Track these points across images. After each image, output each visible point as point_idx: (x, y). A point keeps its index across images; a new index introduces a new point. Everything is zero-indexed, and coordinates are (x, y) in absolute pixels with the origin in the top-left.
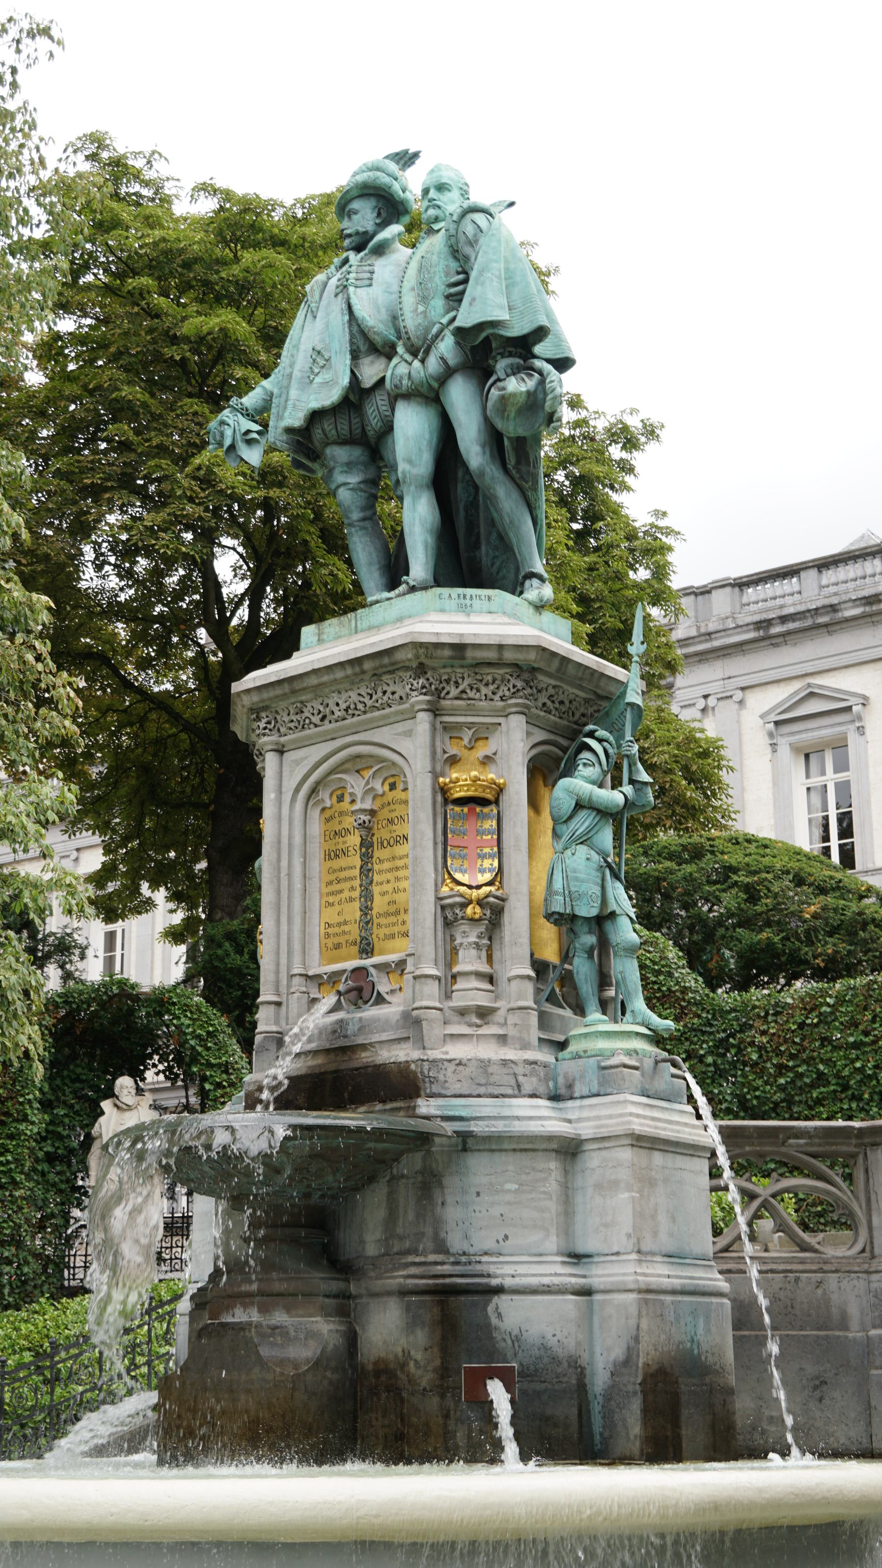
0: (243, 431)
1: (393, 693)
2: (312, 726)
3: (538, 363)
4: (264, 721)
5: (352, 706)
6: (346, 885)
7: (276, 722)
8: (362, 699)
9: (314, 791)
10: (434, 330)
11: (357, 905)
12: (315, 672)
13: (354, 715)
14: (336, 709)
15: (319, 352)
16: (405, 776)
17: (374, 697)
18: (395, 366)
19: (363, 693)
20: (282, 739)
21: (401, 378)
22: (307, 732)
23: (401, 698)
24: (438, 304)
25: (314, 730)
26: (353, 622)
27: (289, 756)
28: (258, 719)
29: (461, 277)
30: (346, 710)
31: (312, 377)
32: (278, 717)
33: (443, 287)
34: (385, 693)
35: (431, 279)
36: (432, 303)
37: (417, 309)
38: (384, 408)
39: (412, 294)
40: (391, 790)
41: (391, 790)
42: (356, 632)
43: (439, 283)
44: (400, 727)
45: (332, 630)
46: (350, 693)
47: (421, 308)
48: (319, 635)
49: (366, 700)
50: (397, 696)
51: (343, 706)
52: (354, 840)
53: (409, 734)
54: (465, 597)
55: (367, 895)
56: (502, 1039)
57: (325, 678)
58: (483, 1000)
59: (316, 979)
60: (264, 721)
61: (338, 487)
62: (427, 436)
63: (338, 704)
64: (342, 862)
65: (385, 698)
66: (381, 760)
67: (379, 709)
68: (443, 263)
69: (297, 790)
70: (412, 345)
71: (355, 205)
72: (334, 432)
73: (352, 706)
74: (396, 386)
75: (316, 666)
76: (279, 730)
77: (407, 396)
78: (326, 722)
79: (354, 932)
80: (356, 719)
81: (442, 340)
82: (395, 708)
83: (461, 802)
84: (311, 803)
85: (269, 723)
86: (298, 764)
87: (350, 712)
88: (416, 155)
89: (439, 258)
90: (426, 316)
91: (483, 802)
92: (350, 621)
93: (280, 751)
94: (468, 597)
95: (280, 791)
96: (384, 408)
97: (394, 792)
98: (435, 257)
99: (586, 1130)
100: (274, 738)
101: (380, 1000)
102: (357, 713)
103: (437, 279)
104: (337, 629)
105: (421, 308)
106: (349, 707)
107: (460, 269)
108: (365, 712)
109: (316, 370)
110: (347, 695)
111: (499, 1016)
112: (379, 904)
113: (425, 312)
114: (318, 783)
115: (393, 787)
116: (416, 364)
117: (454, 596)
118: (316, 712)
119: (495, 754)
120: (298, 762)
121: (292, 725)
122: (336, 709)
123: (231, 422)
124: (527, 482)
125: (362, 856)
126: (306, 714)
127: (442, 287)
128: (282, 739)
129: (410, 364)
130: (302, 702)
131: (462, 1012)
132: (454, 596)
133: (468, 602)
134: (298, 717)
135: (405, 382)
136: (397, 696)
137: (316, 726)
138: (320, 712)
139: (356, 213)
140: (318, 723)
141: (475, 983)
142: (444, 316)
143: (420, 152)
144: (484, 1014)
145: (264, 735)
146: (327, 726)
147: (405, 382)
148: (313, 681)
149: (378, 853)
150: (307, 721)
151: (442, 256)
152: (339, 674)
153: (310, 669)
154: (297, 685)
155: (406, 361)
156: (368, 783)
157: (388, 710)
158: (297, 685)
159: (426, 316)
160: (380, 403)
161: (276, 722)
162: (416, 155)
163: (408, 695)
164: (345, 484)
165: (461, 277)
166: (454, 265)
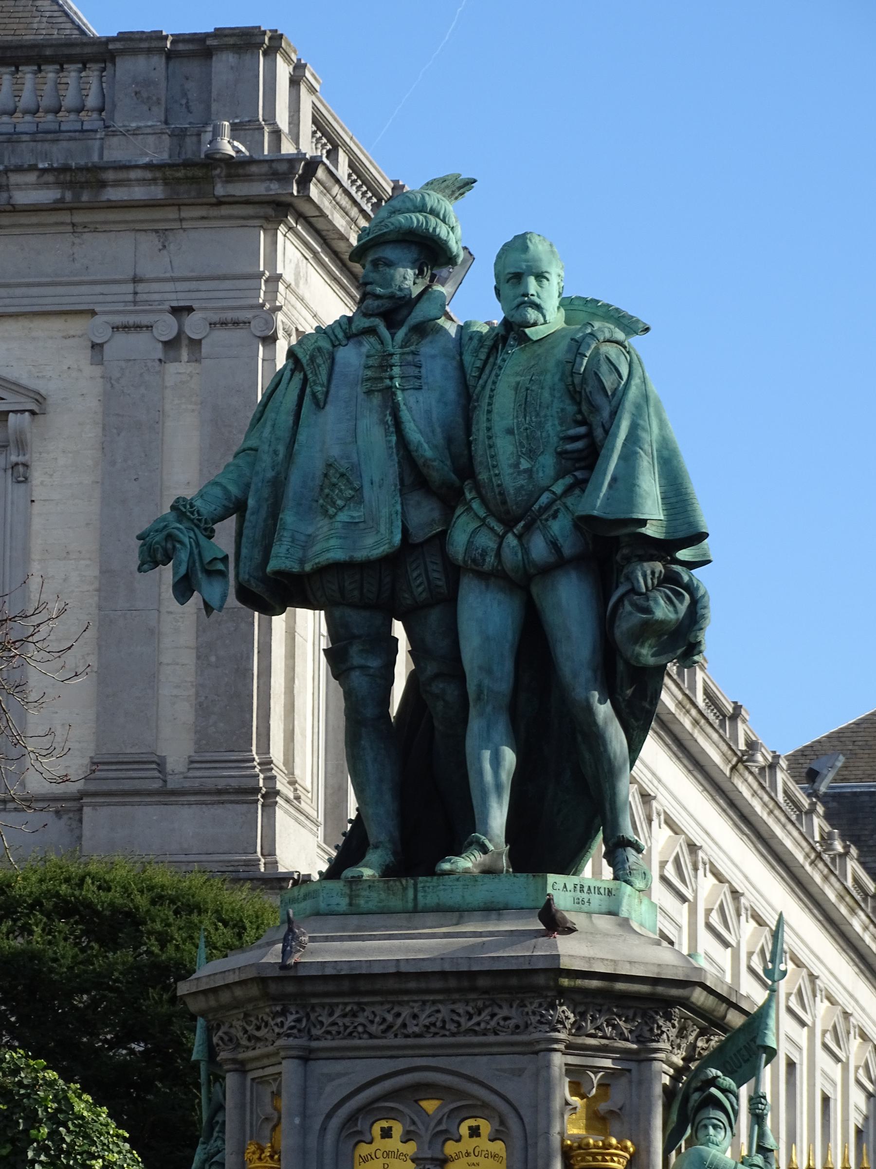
0: (207, 558)
1: (506, 1019)
2: (365, 1036)
4: (291, 1018)
5: (439, 1024)
7: (308, 1019)
8: (456, 1018)
9: (352, 1118)
10: (545, 499)
12: (398, 975)
13: (435, 1034)
14: (411, 1023)
15: (342, 475)
16: (502, 1123)
17: (476, 1019)
18: (474, 532)
19: (461, 1011)
20: (314, 1044)
21: (484, 553)
22: (357, 1042)
23: (517, 1027)
24: (547, 462)
25: (365, 1042)
26: (411, 893)
28: (284, 1013)
29: (582, 430)
30: (427, 1027)
31: (332, 511)
32: (313, 1016)
33: (555, 439)
34: (493, 1015)
35: (540, 426)
36: (541, 459)
37: (517, 465)
38: (436, 575)
39: (509, 438)
40: (471, 1136)
41: (471, 1136)
42: (415, 910)
43: (551, 432)
44: (506, 1062)
45: (374, 895)
46: (440, 1007)
47: (525, 464)
48: (351, 897)
49: (462, 1020)
50: (512, 1023)
51: (424, 1020)
54: (582, 887)
57: (412, 985)
60: (291, 1018)
61: (353, 668)
62: (510, 636)
63: (415, 1016)
65: (493, 1023)
67: (476, 1033)
68: (557, 405)
69: (329, 1116)
70: (508, 512)
71: (389, 253)
72: (356, 593)
73: (439, 1024)
74: (474, 561)
75: (404, 969)
76: (309, 1031)
77: (483, 576)
78: (390, 1035)
80: (438, 1040)
81: (555, 516)
82: (501, 1038)
84: (344, 1134)
85: (299, 1020)
86: (333, 1080)
87: (433, 1029)
88: (469, 183)
89: (553, 396)
90: (531, 477)
92: (405, 889)
93: (306, 1057)
94: (586, 889)
95: (304, 1116)
96: (436, 575)
97: (475, 1139)
98: (546, 394)
100: (302, 1042)
102: (443, 1032)
103: (549, 426)
104: (383, 896)
105: (525, 464)
106: (434, 1025)
107: (579, 417)
108: (453, 1035)
109: (340, 503)
110: (434, 1008)
113: (529, 472)
114: (359, 1110)
116: (511, 540)
117: (570, 887)
118: (377, 1019)
119: (620, 1109)
120: (331, 1078)
121: (334, 1029)
122: (411, 1023)
123: (186, 540)
124: (637, 720)
126: (361, 1019)
127: (554, 440)
128: (314, 1044)
129: (502, 538)
130: (359, 1004)
132: (570, 887)
133: (585, 896)
134: (347, 1021)
135: (490, 560)
136: (512, 1023)
137: (371, 1036)
138: (384, 1020)
139: (390, 264)
140: (380, 1034)
142: (556, 480)
143: (475, 181)
145: (289, 1036)
146: (390, 1040)
147: (490, 560)
148: (391, 984)
150: (360, 1029)
151: (557, 395)
152: (437, 984)
153: (392, 970)
154: (363, 985)
155: (492, 529)
156: (440, 1122)
157: (491, 1038)
158: (363, 985)
159: (531, 477)
160: (431, 567)
161: (308, 1019)
162: (469, 183)
163: (527, 1026)
164: (362, 668)
165: (582, 430)
166: (571, 409)
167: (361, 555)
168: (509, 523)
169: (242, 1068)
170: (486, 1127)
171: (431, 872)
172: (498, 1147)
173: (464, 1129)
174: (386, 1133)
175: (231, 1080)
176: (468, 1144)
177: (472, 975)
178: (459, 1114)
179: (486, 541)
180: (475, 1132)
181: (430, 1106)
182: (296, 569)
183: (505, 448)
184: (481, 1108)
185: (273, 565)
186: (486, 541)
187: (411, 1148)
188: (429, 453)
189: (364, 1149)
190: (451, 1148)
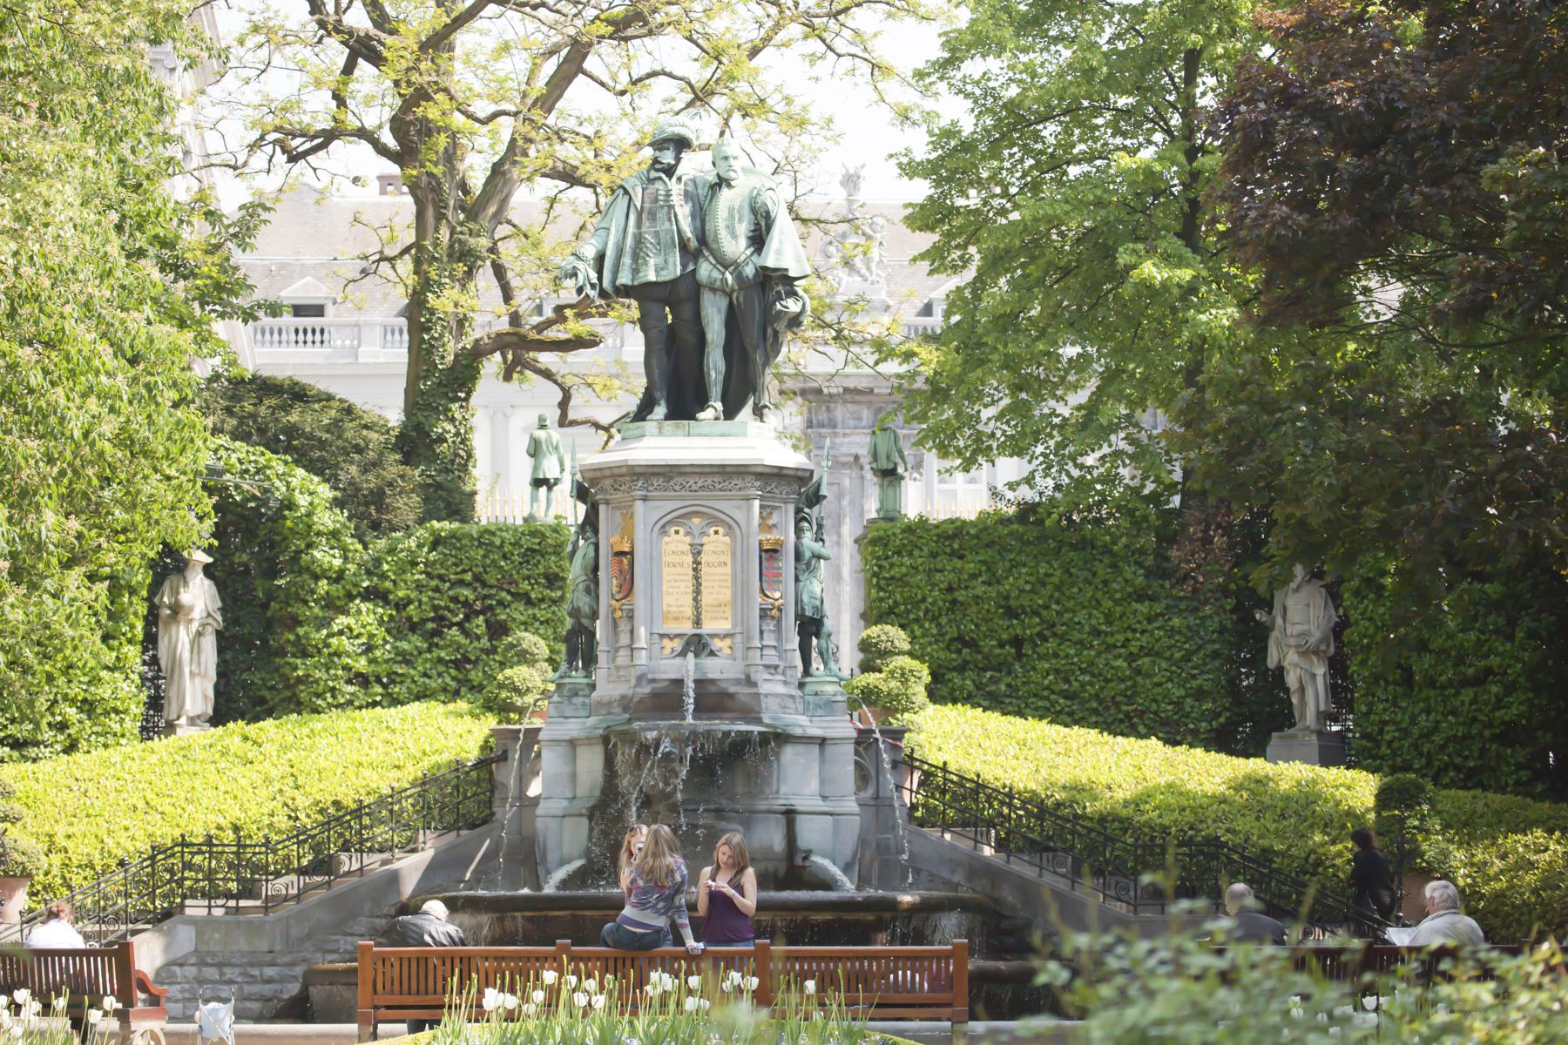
3: (800, 291)
6: (682, 585)
11: (690, 597)
27: (650, 504)
52: (690, 559)
53: (739, 508)
55: (697, 592)
56: (785, 683)
58: (777, 662)
59: (662, 636)
64: (679, 570)
66: (712, 516)
77: (713, 290)
79: (689, 611)
83: (767, 551)
91: (775, 551)
93: (645, 499)
99: (829, 733)
101: (712, 653)
111: (780, 670)
112: (706, 599)
115: (716, 532)
116: (728, 276)
120: (655, 508)
125: (695, 570)
131: (767, 667)
141: (773, 652)
144: (776, 667)
149: (704, 569)
167: (661, 279)
168: (726, 268)
169: (607, 503)
170: (721, 530)
171: (693, 418)
172: (727, 539)
173: (712, 531)
174: (677, 532)
175: (602, 508)
176: (713, 537)
177: (724, 466)
178: (709, 525)
179: (716, 275)
180: (716, 532)
181: (696, 521)
182: (629, 283)
183: (723, 234)
184: (721, 522)
185: (618, 282)
186: (716, 275)
187: (688, 539)
188: (690, 235)
189: (666, 539)
190: (705, 539)
